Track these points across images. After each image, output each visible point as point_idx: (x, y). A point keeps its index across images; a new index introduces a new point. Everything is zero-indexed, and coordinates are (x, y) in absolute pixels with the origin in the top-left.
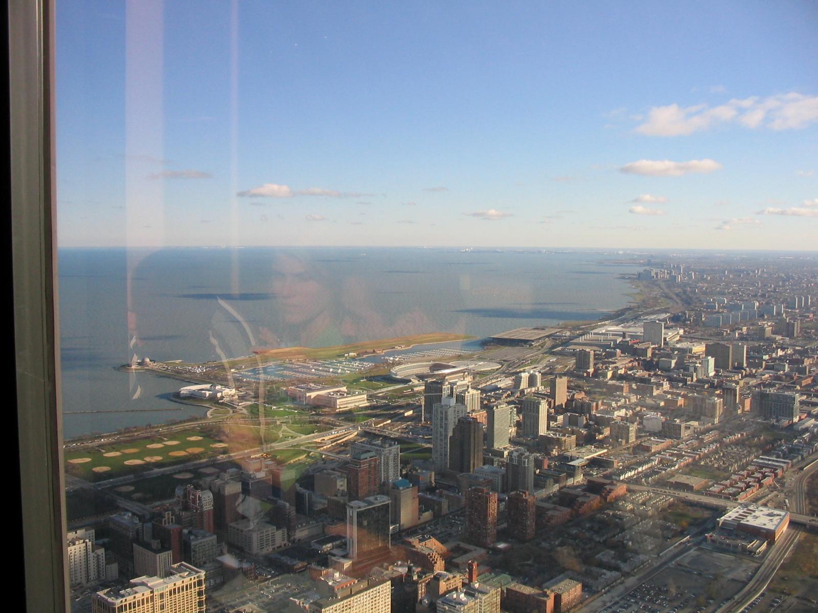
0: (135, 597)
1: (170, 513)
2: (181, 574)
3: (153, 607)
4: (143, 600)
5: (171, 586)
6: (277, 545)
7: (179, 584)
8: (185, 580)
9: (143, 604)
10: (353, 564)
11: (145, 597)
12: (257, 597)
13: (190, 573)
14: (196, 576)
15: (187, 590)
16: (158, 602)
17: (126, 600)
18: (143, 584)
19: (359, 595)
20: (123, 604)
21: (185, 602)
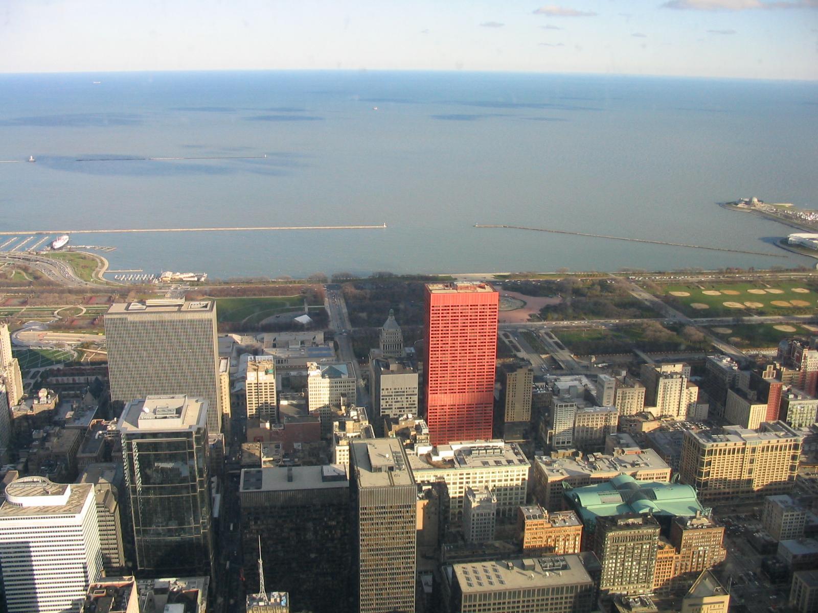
0: (726, 445)
1: (772, 366)
2: (777, 433)
3: (743, 459)
4: (734, 449)
5: (764, 443)
7: (774, 442)
9: (734, 453)
11: (736, 447)
13: (786, 434)
14: (793, 439)
15: (781, 450)
16: (748, 454)
17: (717, 445)
18: (736, 433)
20: (714, 448)
21: (777, 462)
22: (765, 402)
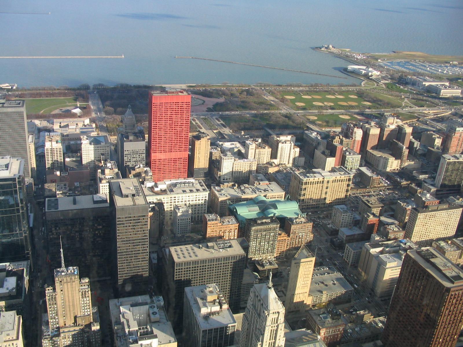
1: (338, 137)
2: (340, 173)
5: (334, 178)
6: (393, 168)
7: (338, 178)
8: (342, 176)
10: (437, 191)
12: (377, 195)
13: (345, 173)
14: (348, 176)
15: (342, 182)
16: (325, 185)
19: (442, 211)
20: (308, 181)
22: (334, 156)
